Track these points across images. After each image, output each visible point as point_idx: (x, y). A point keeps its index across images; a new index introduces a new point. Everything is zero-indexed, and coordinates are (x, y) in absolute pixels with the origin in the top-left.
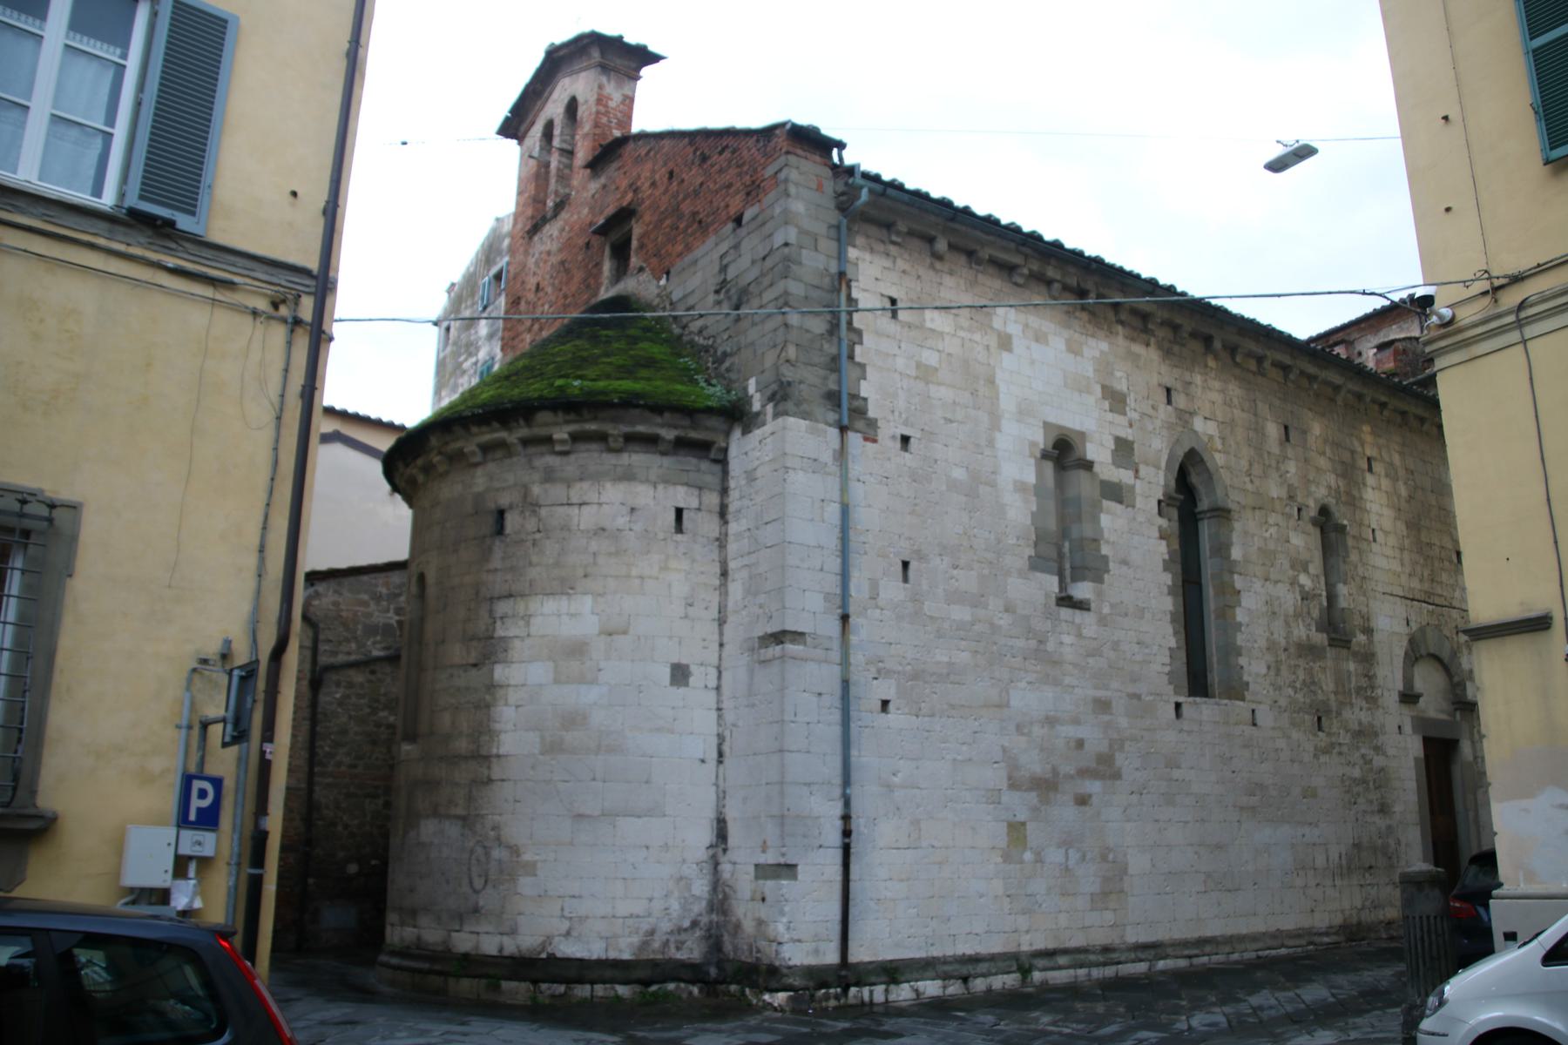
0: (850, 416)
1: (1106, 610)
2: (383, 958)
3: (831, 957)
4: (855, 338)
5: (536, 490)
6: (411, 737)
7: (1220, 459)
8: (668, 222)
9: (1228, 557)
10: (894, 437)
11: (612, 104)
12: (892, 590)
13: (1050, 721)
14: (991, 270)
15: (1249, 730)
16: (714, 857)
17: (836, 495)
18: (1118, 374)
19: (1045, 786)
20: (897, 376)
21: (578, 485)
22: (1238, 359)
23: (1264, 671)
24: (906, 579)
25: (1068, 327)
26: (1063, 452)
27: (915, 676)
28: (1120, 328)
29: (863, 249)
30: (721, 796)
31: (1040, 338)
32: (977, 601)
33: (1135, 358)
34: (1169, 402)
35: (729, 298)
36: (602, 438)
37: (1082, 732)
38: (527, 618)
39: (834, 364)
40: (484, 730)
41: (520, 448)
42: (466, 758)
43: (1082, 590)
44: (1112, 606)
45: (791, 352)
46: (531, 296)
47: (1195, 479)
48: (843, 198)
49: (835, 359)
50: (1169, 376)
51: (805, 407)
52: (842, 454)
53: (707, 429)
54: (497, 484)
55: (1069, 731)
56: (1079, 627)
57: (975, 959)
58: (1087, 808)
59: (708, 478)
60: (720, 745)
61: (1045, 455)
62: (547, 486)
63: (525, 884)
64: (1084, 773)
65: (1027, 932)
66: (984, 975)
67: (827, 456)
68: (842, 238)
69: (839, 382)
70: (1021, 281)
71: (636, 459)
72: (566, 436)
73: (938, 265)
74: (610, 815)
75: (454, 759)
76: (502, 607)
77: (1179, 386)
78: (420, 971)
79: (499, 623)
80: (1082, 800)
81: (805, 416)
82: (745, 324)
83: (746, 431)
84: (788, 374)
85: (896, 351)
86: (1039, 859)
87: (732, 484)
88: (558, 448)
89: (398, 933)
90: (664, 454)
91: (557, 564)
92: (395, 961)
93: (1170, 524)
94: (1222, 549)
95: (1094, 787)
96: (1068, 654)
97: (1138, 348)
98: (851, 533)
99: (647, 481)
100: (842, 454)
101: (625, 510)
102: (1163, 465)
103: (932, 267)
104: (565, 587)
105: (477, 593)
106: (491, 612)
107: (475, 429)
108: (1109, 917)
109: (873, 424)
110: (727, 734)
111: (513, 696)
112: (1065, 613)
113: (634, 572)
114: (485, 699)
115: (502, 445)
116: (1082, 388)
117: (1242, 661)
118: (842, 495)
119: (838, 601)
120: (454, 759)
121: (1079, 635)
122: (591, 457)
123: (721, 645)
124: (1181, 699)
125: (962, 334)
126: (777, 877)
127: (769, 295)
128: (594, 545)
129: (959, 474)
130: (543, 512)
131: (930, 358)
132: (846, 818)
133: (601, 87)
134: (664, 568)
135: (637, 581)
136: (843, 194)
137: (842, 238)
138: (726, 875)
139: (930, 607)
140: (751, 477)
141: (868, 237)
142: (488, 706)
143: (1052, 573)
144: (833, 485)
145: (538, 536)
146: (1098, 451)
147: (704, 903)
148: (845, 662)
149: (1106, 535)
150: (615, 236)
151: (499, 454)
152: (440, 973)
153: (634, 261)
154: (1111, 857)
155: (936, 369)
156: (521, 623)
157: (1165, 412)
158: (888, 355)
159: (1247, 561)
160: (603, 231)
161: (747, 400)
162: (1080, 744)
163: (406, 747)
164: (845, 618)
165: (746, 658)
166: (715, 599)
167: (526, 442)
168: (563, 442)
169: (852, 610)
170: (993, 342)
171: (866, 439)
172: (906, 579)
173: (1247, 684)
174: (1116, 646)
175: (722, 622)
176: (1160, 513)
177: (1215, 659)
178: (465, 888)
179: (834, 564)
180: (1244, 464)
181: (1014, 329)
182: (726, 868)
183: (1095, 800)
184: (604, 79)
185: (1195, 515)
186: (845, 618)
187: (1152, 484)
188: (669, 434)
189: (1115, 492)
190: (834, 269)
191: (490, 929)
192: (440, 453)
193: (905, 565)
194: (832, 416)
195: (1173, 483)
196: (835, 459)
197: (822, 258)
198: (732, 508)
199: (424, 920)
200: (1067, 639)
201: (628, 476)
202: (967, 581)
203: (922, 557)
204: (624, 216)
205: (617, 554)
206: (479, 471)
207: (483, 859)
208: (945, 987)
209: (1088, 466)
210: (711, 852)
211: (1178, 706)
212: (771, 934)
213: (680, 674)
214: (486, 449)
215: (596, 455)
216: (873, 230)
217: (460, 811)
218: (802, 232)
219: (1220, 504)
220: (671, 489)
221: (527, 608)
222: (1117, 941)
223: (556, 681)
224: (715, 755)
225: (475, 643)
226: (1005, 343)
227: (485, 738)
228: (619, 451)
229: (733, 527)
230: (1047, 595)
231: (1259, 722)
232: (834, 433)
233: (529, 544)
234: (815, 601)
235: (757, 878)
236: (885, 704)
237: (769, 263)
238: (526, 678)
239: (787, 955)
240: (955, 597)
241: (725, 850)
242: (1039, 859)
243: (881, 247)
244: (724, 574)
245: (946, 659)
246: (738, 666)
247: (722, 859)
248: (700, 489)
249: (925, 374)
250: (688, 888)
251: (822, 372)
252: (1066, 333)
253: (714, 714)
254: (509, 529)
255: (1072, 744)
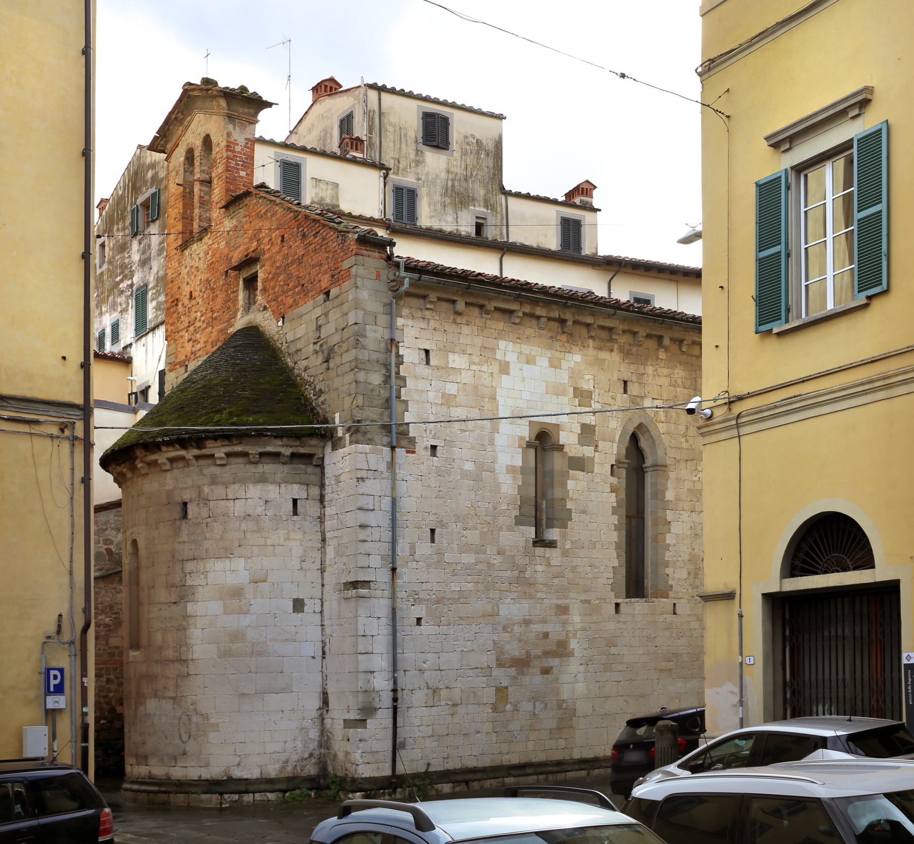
0: (397, 437)
1: (568, 546)
2: (125, 786)
3: (387, 772)
4: (401, 383)
5: (206, 489)
6: (136, 646)
7: (662, 428)
8: (281, 277)
9: (663, 499)
10: (426, 448)
11: (238, 149)
12: (425, 548)
13: (527, 622)
14: (497, 315)
15: (671, 617)
16: (321, 715)
17: (389, 493)
18: (587, 377)
19: (521, 664)
20: (429, 405)
21: (232, 486)
22: (684, 349)
23: (685, 576)
24: (433, 541)
25: (551, 348)
26: (543, 441)
27: (438, 602)
28: (591, 341)
29: (407, 317)
30: (325, 679)
31: (530, 360)
32: (479, 550)
33: (600, 362)
34: (625, 392)
35: (323, 352)
36: (245, 455)
37: (547, 628)
38: (205, 573)
39: (387, 404)
40: (182, 643)
41: (194, 462)
42: (173, 661)
43: (553, 534)
44: (572, 543)
45: (360, 400)
46: (186, 302)
47: (643, 444)
48: (394, 284)
49: (388, 400)
50: (626, 371)
51: (369, 436)
52: (391, 465)
53: (311, 446)
54: (181, 485)
55: (537, 628)
56: (548, 559)
57: (474, 771)
58: (549, 676)
59: (313, 478)
60: (323, 647)
61: (529, 445)
62: (213, 487)
63: (213, 737)
64: (547, 654)
65: (507, 753)
66: (479, 780)
67: (383, 467)
68: (391, 313)
69: (390, 416)
70: (517, 321)
71: (268, 468)
72: (223, 455)
73: (459, 320)
74: (260, 693)
75: (166, 662)
76: (189, 566)
77: (634, 378)
78: (152, 792)
79: (188, 577)
80: (546, 671)
81: (370, 441)
82: (332, 373)
83: (334, 448)
84: (359, 415)
85: (429, 388)
86: (516, 709)
87: (327, 482)
88: (218, 462)
89: (134, 769)
90: (284, 464)
91: (222, 538)
92: (135, 787)
93: (620, 481)
94: (659, 495)
95: (554, 662)
96: (540, 578)
97: (604, 355)
98: (398, 515)
99: (275, 482)
100: (391, 465)
101: (262, 503)
102: (617, 439)
103: (455, 322)
104: (227, 553)
105: (173, 557)
106: (183, 569)
107: (164, 449)
108: (562, 743)
109: (412, 441)
110: (327, 641)
111: (200, 622)
112: (539, 551)
113: (269, 543)
114: (183, 624)
115: (182, 458)
116: (558, 391)
117: (669, 571)
118: (392, 492)
119: (390, 560)
120: (166, 662)
121: (549, 565)
122: (238, 467)
123: (323, 585)
124: (619, 601)
125: (474, 367)
126: (355, 727)
127: (347, 357)
128: (244, 526)
129: (469, 466)
130: (212, 504)
131: (451, 389)
132: (395, 691)
133: (229, 135)
134: (287, 539)
135: (271, 548)
136: (393, 281)
137: (391, 313)
138: (328, 726)
139: (448, 557)
140: (337, 478)
141: (410, 308)
142: (185, 629)
143: (530, 525)
144: (387, 484)
145: (209, 520)
146: (568, 438)
147: (316, 743)
148: (393, 597)
149: (571, 494)
150: (246, 273)
151: (181, 464)
152: (165, 792)
153: (260, 299)
154: (564, 706)
155: (455, 396)
156: (202, 576)
157: (622, 400)
158: (423, 391)
159: (677, 499)
160: (239, 268)
161: (334, 430)
162: (546, 635)
163: (133, 654)
164: (394, 570)
165: (336, 595)
166: (318, 555)
167: (197, 457)
168: (221, 458)
169: (398, 563)
170: (495, 368)
171: (408, 452)
172: (433, 541)
173: (671, 586)
174: (574, 569)
175: (323, 571)
176: (612, 474)
177: (649, 570)
178: (177, 741)
179: (388, 536)
180: (682, 428)
181: (511, 357)
182: (328, 721)
183: (555, 670)
184: (231, 127)
185: (643, 469)
186: (394, 570)
187: (609, 451)
188: (287, 451)
189: (579, 464)
190: (387, 336)
191: (193, 764)
192: (142, 461)
193: (433, 531)
194: (386, 440)
195: (624, 452)
196: (388, 468)
197: (380, 329)
198: (327, 498)
199: (152, 761)
200: (540, 568)
201: (262, 480)
202: (473, 537)
203: (442, 524)
204: (250, 261)
205: (258, 531)
206: (169, 475)
207: (187, 722)
208: (454, 788)
209: (561, 448)
210: (319, 712)
211: (617, 605)
212: (353, 760)
213: (298, 605)
214: (172, 460)
215: (242, 466)
216: (414, 302)
217: (172, 694)
218: (366, 313)
219: (660, 463)
220: (289, 486)
221: (205, 567)
222: (567, 758)
223: (225, 613)
224: (321, 654)
225: (174, 589)
226: (505, 368)
227: (184, 649)
228: (257, 463)
229: (328, 511)
230: (527, 541)
231: (678, 612)
232: (387, 450)
233: (204, 525)
234: (375, 561)
235: (345, 727)
236: (419, 620)
237: (346, 334)
238: (207, 614)
239: (361, 772)
240: (465, 548)
241: (327, 711)
242: (516, 709)
243: (419, 314)
244: (324, 540)
245: (458, 589)
246: (333, 599)
247: (326, 716)
248: (308, 485)
249: (448, 400)
250: (307, 733)
251: (379, 411)
252: (549, 354)
253: (320, 628)
254: (190, 516)
255: (541, 636)
